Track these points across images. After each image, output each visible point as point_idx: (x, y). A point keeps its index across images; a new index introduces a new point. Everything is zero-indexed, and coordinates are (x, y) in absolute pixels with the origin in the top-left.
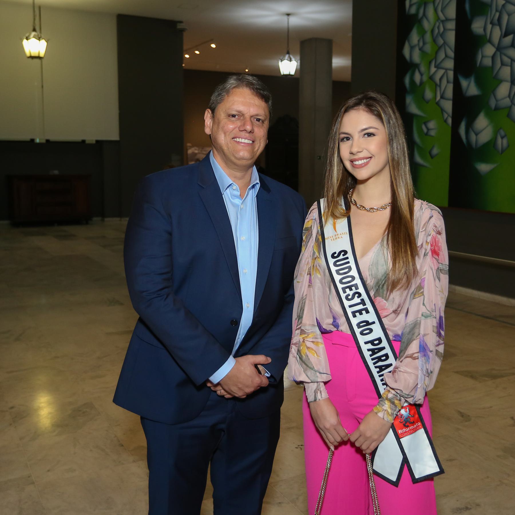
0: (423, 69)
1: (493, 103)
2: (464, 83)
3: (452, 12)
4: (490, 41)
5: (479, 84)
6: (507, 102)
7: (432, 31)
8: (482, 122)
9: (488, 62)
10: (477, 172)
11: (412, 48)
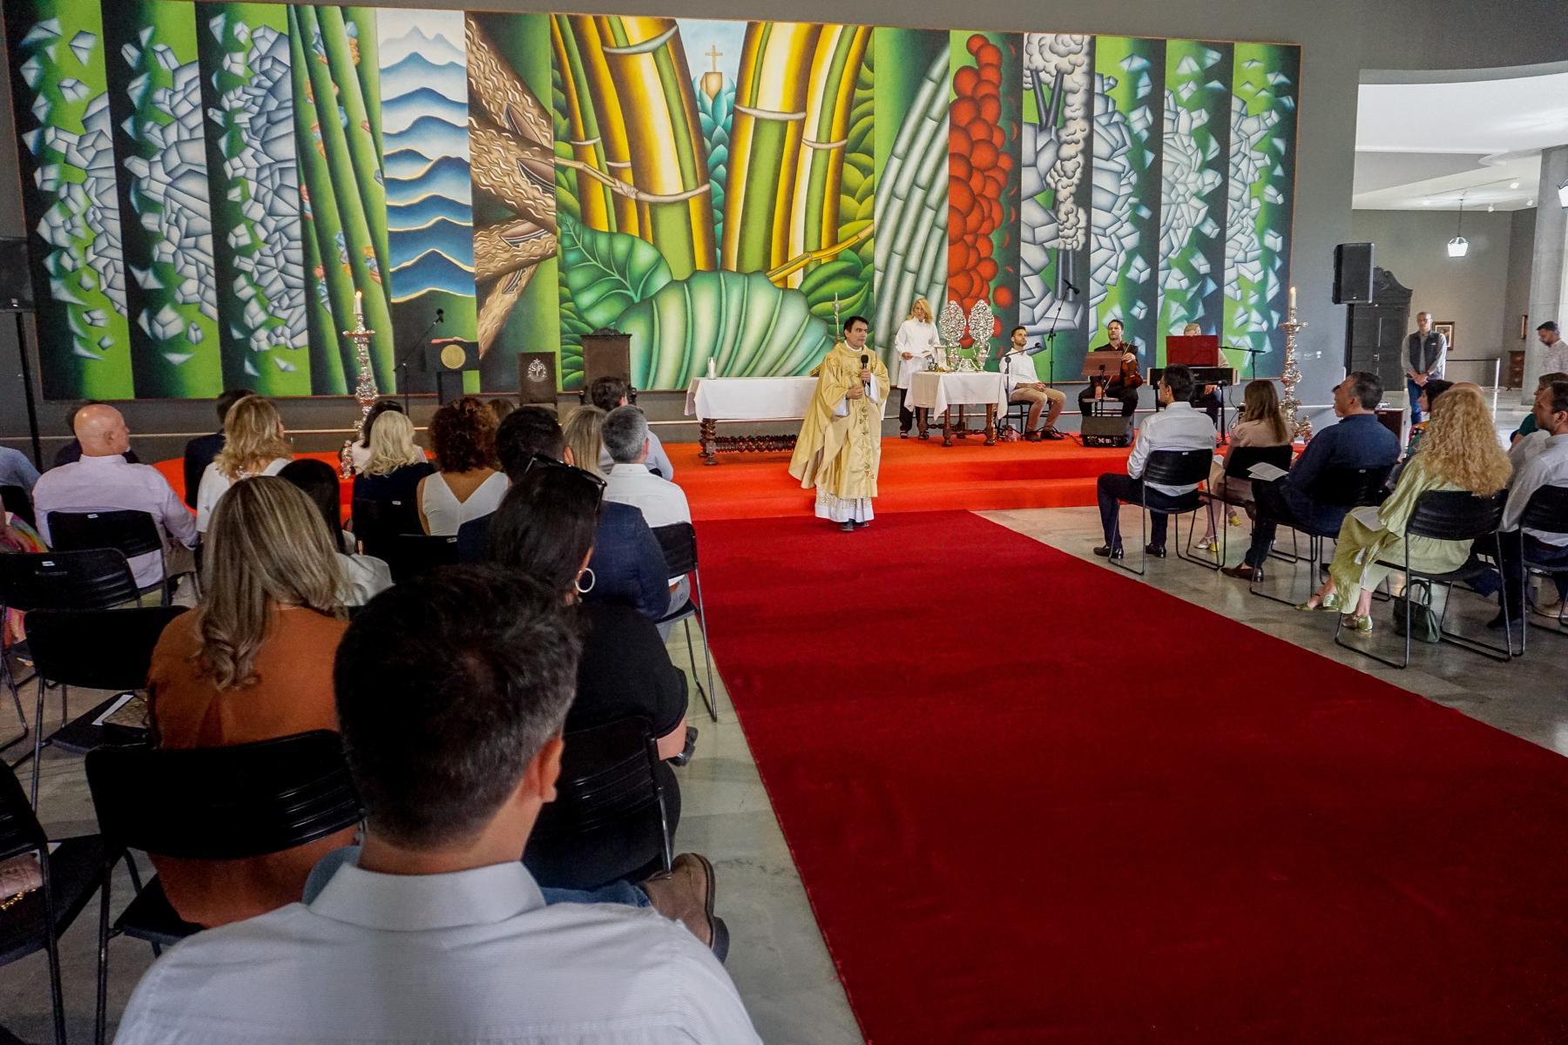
0: (75, 253)
1: (179, 298)
2: (139, 275)
3: (112, 200)
4: (168, 239)
5: (159, 275)
6: (197, 298)
7: (85, 215)
8: (167, 314)
9: (170, 259)
10: (169, 363)
11: (53, 229)
